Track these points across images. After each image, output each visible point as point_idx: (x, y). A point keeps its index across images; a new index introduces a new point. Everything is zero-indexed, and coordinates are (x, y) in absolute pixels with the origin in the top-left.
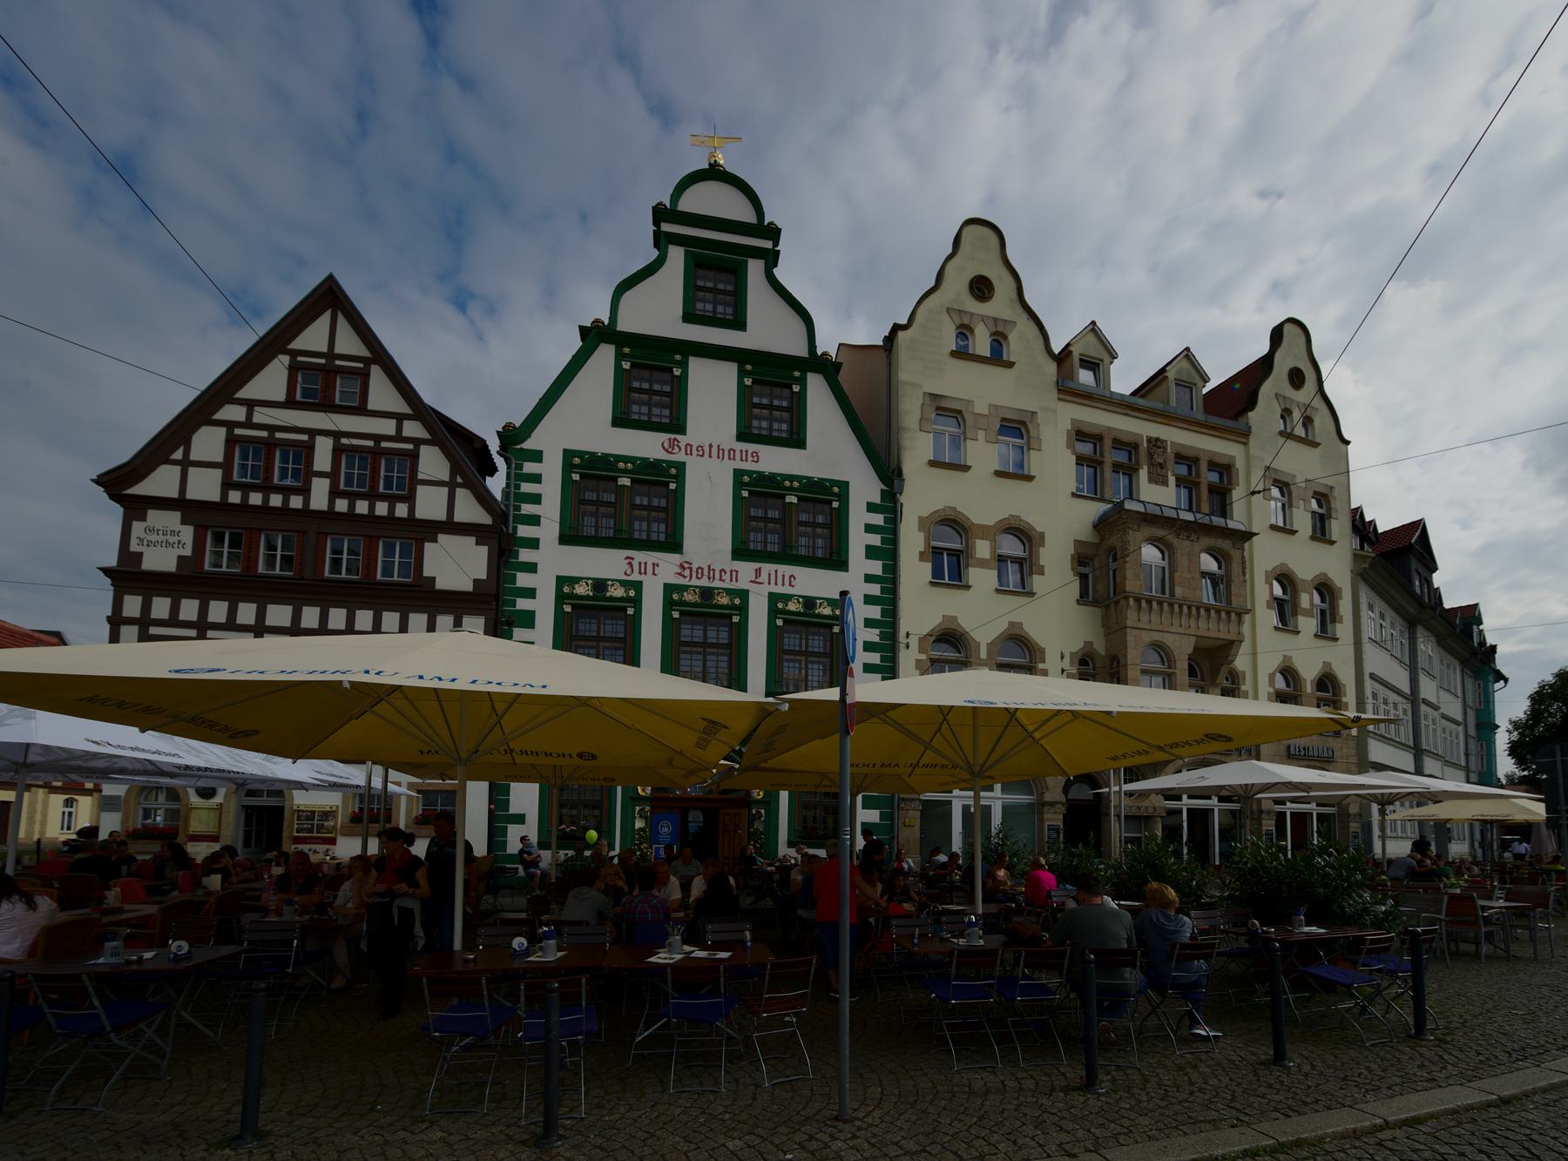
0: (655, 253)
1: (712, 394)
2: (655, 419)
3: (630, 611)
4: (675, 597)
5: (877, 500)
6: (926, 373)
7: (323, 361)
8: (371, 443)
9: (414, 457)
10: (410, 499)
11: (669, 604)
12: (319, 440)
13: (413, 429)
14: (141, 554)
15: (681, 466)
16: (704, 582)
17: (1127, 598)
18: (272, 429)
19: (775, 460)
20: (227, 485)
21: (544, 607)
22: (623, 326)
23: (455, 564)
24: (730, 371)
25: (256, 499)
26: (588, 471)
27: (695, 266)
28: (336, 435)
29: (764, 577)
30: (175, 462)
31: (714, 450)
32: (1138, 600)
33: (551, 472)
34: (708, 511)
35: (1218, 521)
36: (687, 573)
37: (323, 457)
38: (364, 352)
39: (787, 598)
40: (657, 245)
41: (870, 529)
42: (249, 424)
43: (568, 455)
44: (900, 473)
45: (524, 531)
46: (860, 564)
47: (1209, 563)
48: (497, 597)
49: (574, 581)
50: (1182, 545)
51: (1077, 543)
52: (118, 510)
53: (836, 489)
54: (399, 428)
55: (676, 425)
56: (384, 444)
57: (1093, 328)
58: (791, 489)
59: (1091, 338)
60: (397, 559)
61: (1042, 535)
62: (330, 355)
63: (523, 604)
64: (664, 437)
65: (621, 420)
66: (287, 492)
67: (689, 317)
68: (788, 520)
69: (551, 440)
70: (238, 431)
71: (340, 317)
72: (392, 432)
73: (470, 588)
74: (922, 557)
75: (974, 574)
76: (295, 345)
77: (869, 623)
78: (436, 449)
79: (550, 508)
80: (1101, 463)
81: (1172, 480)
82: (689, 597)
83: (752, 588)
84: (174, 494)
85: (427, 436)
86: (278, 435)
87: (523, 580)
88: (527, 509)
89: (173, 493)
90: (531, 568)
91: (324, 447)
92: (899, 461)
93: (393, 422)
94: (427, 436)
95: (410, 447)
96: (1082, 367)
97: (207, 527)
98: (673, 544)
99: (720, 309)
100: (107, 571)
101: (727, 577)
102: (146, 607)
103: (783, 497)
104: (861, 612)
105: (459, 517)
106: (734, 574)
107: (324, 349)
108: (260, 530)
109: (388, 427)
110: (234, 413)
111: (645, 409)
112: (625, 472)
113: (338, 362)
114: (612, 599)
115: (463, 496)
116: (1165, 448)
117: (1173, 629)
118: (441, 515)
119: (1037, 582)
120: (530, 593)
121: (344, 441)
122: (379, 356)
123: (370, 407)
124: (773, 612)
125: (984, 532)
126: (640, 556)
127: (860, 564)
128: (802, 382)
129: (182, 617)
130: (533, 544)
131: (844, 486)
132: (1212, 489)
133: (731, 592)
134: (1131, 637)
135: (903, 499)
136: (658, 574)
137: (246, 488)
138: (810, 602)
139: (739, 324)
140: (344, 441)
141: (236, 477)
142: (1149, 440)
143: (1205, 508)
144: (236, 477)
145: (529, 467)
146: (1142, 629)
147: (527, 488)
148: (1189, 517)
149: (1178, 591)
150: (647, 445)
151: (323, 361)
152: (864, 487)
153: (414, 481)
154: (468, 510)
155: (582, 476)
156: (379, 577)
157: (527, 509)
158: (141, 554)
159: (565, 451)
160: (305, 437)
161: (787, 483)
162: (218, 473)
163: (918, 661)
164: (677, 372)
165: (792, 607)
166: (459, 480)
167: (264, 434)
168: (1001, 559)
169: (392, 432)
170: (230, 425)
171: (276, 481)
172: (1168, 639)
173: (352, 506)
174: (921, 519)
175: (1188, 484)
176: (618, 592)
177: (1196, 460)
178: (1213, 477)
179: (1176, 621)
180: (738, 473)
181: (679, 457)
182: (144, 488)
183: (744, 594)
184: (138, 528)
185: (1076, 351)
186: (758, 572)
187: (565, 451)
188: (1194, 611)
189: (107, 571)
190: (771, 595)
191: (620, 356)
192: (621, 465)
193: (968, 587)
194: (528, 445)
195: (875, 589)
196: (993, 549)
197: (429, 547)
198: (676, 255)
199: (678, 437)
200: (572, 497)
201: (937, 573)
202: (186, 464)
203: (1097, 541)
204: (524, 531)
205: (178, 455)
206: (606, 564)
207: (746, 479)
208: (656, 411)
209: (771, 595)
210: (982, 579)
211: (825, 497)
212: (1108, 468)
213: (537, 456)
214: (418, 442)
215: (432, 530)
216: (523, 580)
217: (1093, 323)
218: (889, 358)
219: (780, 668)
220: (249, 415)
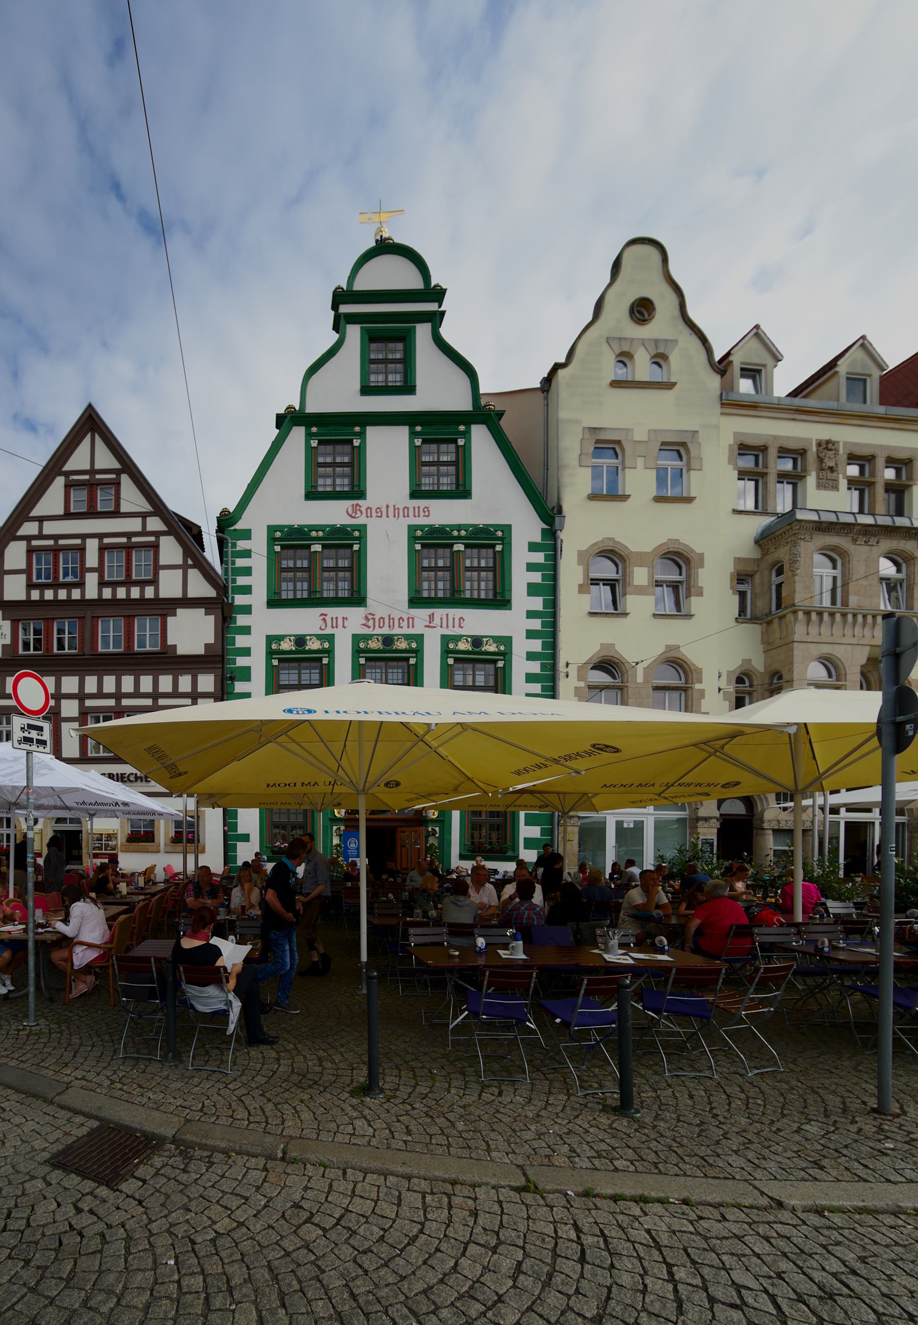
0: (337, 336)
1: (387, 456)
2: (338, 489)
4: (362, 645)
5: (538, 538)
6: (583, 410)
7: (87, 477)
8: (124, 540)
9: (155, 547)
10: (154, 582)
12: (88, 540)
13: (154, 524)
15: (362, 528)
16: (386, 631)
17: (795, 612)
19: (444, 513)
20: (30, 586)
21: (257, 663)
22: (311, 409)
23: (191, 632)
24: (401, 434)
25: (49, 595)
26: (289, 540)
28: (100, 536)
29: (437, 621)
32: (808, 613)
33: (258, 544)
34: (387, 566)
35: (900, 521)
36: (371, 623)
38: (117, 465)
39: (457, 639)
40: (336, 328)
41: (531, 567)
42: (40, 536)
43: (271, 529)
44: (560, 511)
46: (523, 601)
47: (887, 568)
48: (223, 656)
49: (279, 638)
50: (859, 552)
51: (738, 560)
53: (499, 534)
54: (144, 525)
55: (357, 492)
56: (134, 540)
57: (757, 333)
58: (459, 538)
59: (754, 344)
60: (148, 633)
61: (701, 557)
62: (93, 471)
63: (241, 661)
64: (347, 504)
65: (312, 494)
66: (69, 586)
67: (367, 390)
68: (458, 565)
69: (257, 521)
70: (35, 543)
71: (97, 436)
73: (201, 651)
74: (582, 589)
75: (632, 602)
76: (67, 467)
77: (531, 656)
78: (171, 538)
79: (259, 581)
80: (764, 475)
81: (843, 484)
82: (374, 645)
83: (428, 633)
85: (165, 528)
86: (61, 542)
87: (241, 641)
88: (241, 581)
90: (246, 630)
91: (92, 546)
92: (559, 499)
93: (139, 521)
94: (165, 528)
95: (153, 539)
96: (742, 376)
97: (19, 620)
98: (357, 598)
99: (391, 377)
101: (404, 624)
103: (451, 546)
104: (522, 646)
105: (191, 594)
106: (411, 621)
107: (88, 467)
108: (53, 619)
109: (134, 525)
110: (30, 528)
111: (329, 481)
112: (317, 539)
113: (98, 476)
115: (194, 575)
116: (837, 450)
117: (845, 640)
118: (178, 594)
119: (695, 604)
120: (246, 652)
121: (106, 541)
122: (128, 466)
123: (124, 508)
124: (446, 652)
125: (642, 559)
126: (333, 612)
127: (523, 601)
128: (466, 434)
130: (247, 610)
131: (507, 529)
132: (890, 487)
133: (408, 637)
134: (798, 651)
135: (562, 535)
136: (346, 625)
137: (42, 587)
138: (477, 641)
139: (408, 388)
140: (106, 541)
141: (35, 580)
142: (819, 444)
143: (880, 507)
144: (35, 580)
145: (242, 545)
146: (808, 646)
147: (240, 562)
148: (867, 520)
149: (853, 600)
150: (333, 513)
151: (87, 477)
152: (526, 527)
153: (157, 567)
154: (199, 587)
155: (283, 547)
156: (136, 649)
157: (241, 581)
160: (78, 541)
161: (455, 533)
163: (577, 689)
164: (356, 443)
165: (463, 646)
166: (190, 562)
168: (659, 584)
169: (139, 529)
170: (28, 538)
171: (61, 579)
172: (839, 652)
173: (114, 593)
174: (580, 554)
175: (860, 485)
176: (313, 645)
177: (871, 459)
178: (890, 474)
179: (849, 632)
180: (412, 529)
183: (419, 638)
185: (737, 360)
186: (431, 617)
188: (870, 619)
190: (443, 636)
191: (309, 436)
192: (314, 534)
193: (625, 614)
194: (239, 526)
195: (536, 624)
196: (651, 575)
197: (170, 620)
199: (360, 502)
203: (759, 557)
207: (419, 533)
208: (338, 481)
209: (443, 636)
210: (639, 605)
211: (490, 540)
212: (772, 478)
213: (246, 534)
214: (157, 534)
215: (165, 608)
216: (241, 641)
217: (757, 327)
218: (546, 398)
220: (41, 528)
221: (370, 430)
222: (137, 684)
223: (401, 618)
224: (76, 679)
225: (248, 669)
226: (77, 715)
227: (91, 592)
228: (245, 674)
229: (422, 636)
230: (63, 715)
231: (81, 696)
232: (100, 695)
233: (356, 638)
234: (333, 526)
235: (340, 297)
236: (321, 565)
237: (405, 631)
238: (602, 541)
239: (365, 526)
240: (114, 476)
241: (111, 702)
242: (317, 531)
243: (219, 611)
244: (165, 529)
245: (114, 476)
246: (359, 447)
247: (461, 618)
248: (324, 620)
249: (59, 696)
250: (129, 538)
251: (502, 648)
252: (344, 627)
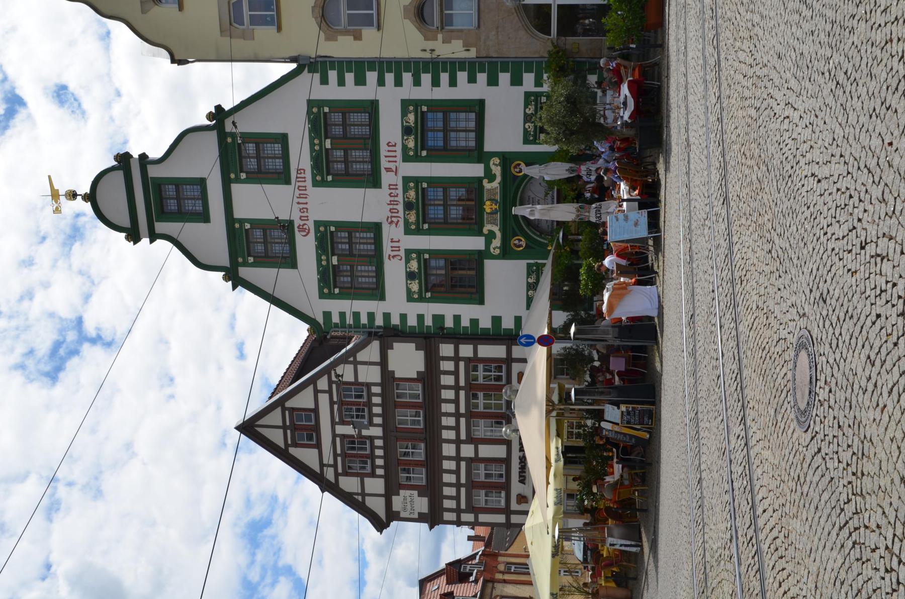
3: (427, 256)
4: (413, 227)
5: (317, 76)
7: (289, 432)
10: (369, 385)
11: (419, 231)
12: (337, 432)
14: (419, 513)
16: (400, 207)
18: (335, 455)
19: (301, 156)
20: (373, 475)
23: (407, 360)
26: (330, 282)
27: (165, 215)
29: (392, 166)
30: (364, 499)
31: (301, 200)
36: (395, 220)
37: (348, 430)
38: (279, 409)
39: (405, 148)
42: (335, 466)
43: (322, 296)
45: (379, 321)
49: (409, 292)
52: (394, 524)
55: (287, 227)
56: (335, 399)
58: (320, 145)
63: (428, 322)
64: (298, 236)
66: (373, 447)
70: (340, 470)
72: (327, 395)
73: (421, 353)
74: (358, 37)
76: (282, 445)
79: (364, 307)
82: (412, 218)
84: (383, 500)
86: (339, 451)
87: (412, 322)
88: (364, 320)
89: (382, 500)
90: (403, 317)
91: (341, 430)
100: (431, 527)
103: (327, 150)
104: (409, 91)
105: (377, 359)
107: (281, 431)
109: (324, 399)
110: (330, 474)
112: (328, 260)
113: (288, 424)
114: (419, 268)
115: (361, 356)
118: (377, 369)
120: (421, 317)
123: (312, 406)
129: (453, 398)
130: (387, 316)
131: (311, 103)
133: (406, 189)
136: (396, 239)
137: (374, 467)
138: (407, 131)
139: (201, 183)
150: (306, 247)
151: (289, 432)
154: (372, 352)
156: (420, 401)
157: (364, 320)
158: (419, 513)
159: (320, 298)
160: (338, 440)
162: (366, 480)
165: (411, 144)
166: (352, 359)
167: (339, 459)
169: (327, 395)
170: (337, 475)
176: (414, 265)
180: (315, 184)
181: (311, 225)
182: (382, 514)
183: (406, 180)
184: (403, 515)
186: (388, 170)
187: (320, 298)
189: (431, 527)
190: (404, 161)
191: (246, 264)
192: (324, 263)
194: (321, 320)
195: (390, 77)
197: (397, 376)
198: (160, 227)
199: (296, 225)
200: (353, 292)
201: (368, 21)
202: (363, 494)
204: (379, 321)
205: (360, 498)
206: (395, 274)
213: (327, 315)
214: (330, 383)
215: (388, 378)
216: (412, 322)
219: (458, 150)
220: (329, 466)
221: (237, 215)
223: (390, 195)
225: (435, 317)
227: (377, 431)
228: (439, 319)
229: (404, 178)
233: (408, 231)
234: (317, 248)
235: (134, 236)
236: (350, 259)
237: (400, 191)
238: (316, 18)
239: (316, 222)
240: (287, 412)
242: (322, 260)
243: (389, 338)
244: (326, 376)
245: (287, 412)
246: (251, 225)
247: (387, 144)
248: (394, 257)
249: (458, 458)
250: (335, 403)
251: (411, 108)
252: (399, 241)
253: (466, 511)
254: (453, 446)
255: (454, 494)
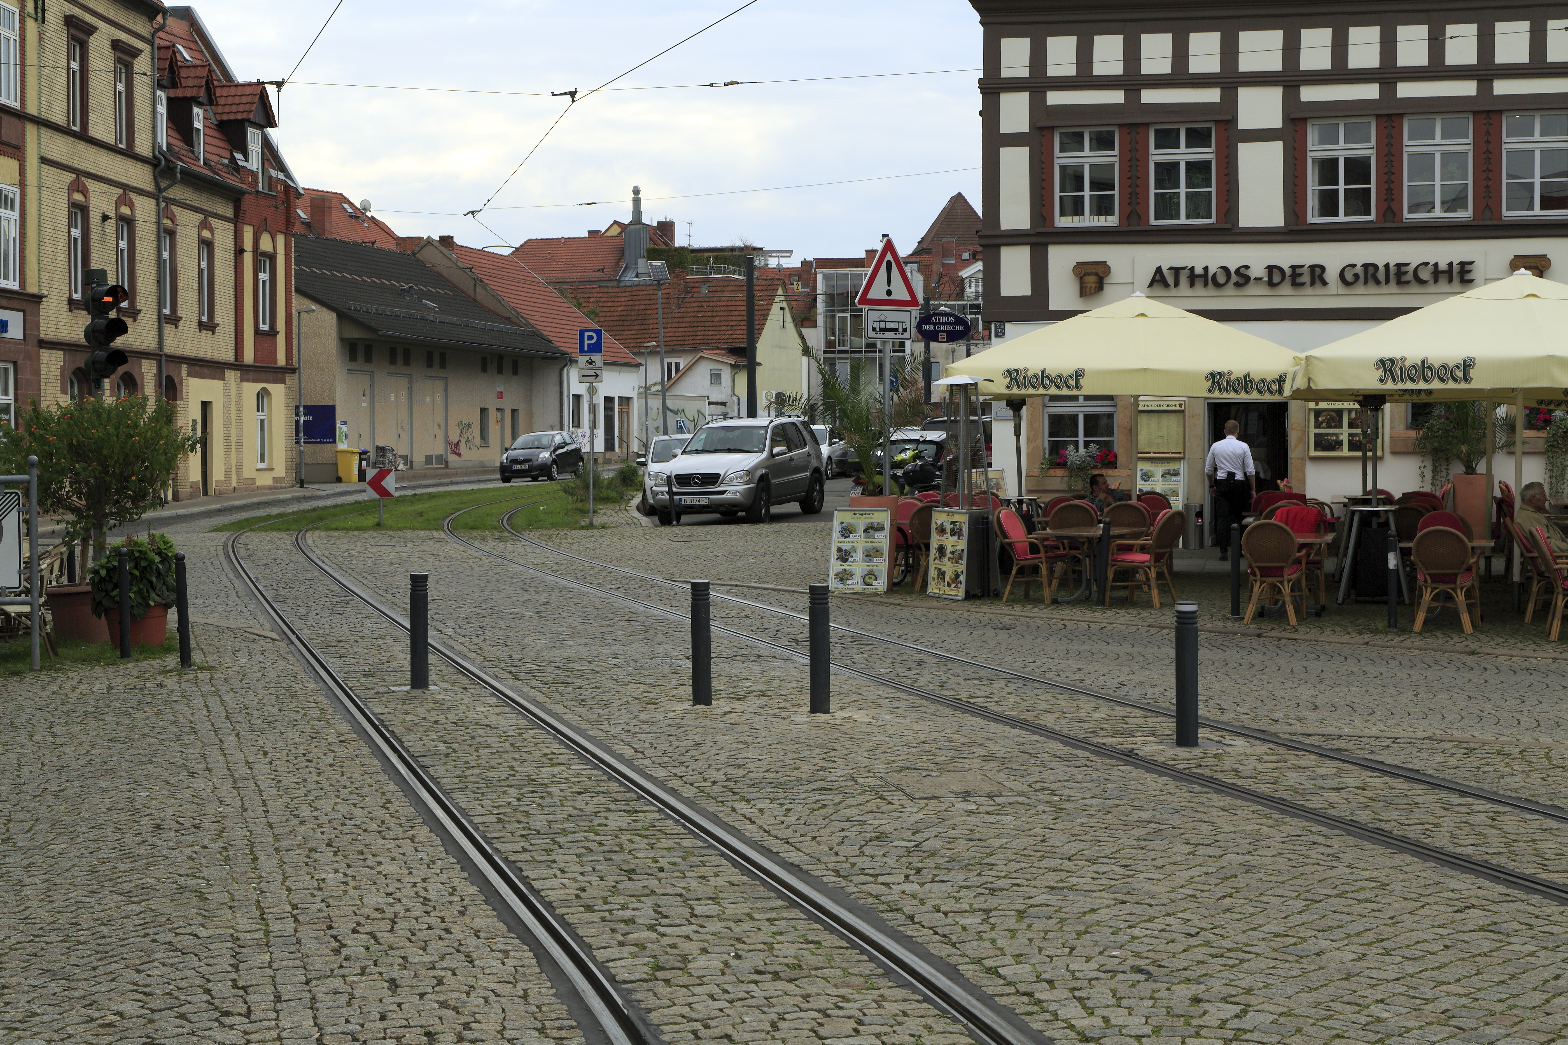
102: (1038, 57)
222: (1340, 48)
224: (1274, 38)
226: (1276, 121)
230: (1244, 123)
231: (1290, 78)
232: (1339, 73)
241: (1370, 91)
249: (1230, 79)
253: (1037, 107)
254: (1274, 63)
255: (1099, 69)
